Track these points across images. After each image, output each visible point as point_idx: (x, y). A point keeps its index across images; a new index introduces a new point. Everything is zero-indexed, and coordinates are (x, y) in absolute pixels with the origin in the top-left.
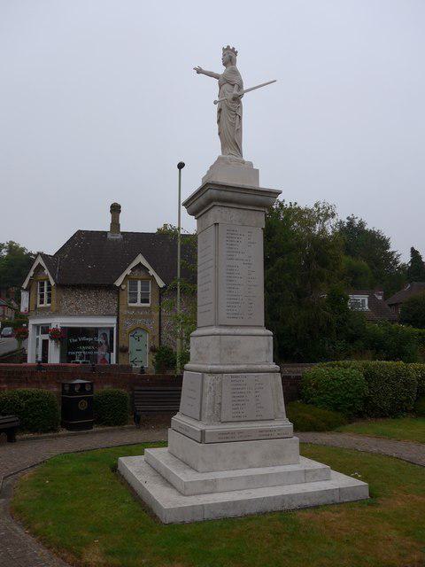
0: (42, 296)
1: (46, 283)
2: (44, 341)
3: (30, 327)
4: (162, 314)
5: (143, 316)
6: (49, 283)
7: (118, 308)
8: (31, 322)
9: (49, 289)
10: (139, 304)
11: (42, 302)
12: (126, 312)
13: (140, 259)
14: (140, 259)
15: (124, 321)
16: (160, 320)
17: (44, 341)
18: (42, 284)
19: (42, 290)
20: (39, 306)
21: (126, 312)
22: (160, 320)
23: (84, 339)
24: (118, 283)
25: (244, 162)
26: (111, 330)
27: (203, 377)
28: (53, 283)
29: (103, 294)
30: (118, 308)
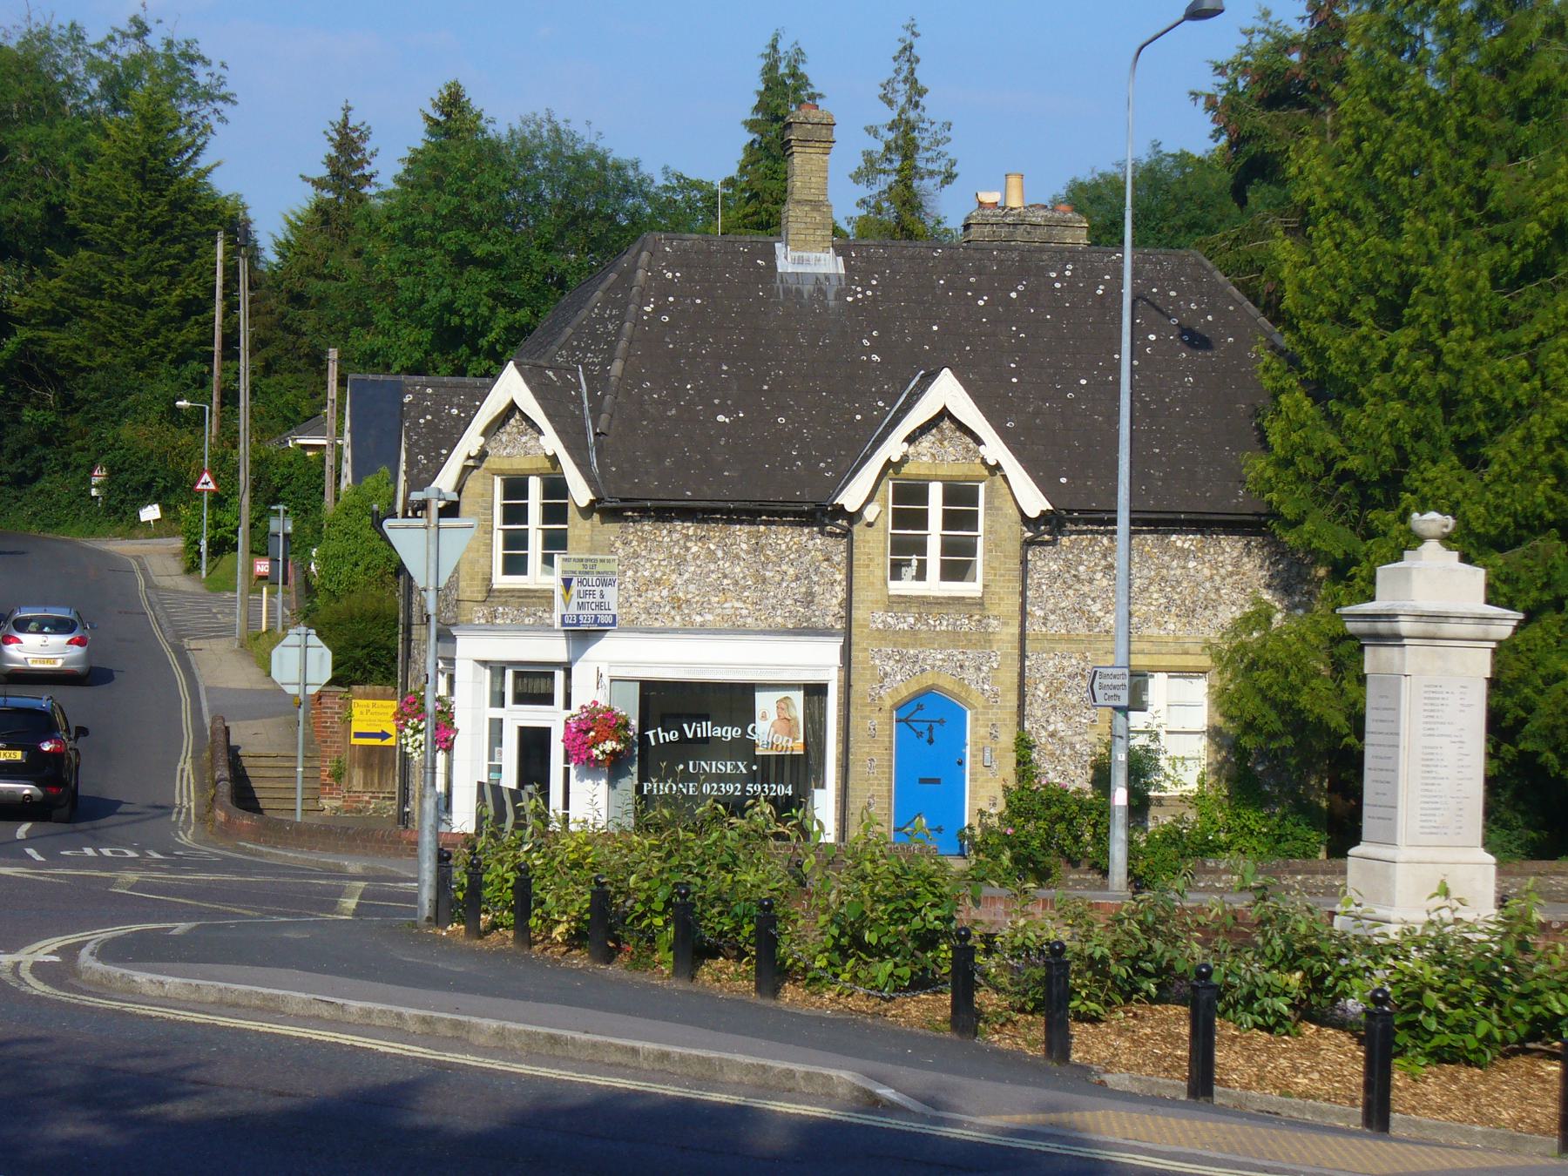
0: (516, 541)
1: (535, 486)
2: (523, 731)
3: (464, 670)
4: (1033, 628)
5: (955, 637)
6: (555, 487)
7: (848, 604)
8: (471, 648)
9: (554, 513)
10: (934, 585)
11: (515, 565)
12: (880, 618)
13: (947, 392)
14: (947, 392)
15: (871, 658)
16: (1023, 656)
17: (523, 731)
18: (516, 487)
19: (515, 514)
20: (501, 581)
21: (880, 618)
22: (1023, 656)
23: (706, 729)
24: (851, 498)
25: (1485, 566)
26: (815, 692)
27: (827, 632)
28: (580, 492)
29: (785, 538)
30: (848, 604)
